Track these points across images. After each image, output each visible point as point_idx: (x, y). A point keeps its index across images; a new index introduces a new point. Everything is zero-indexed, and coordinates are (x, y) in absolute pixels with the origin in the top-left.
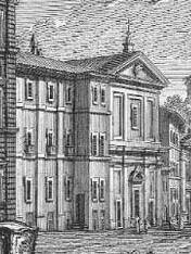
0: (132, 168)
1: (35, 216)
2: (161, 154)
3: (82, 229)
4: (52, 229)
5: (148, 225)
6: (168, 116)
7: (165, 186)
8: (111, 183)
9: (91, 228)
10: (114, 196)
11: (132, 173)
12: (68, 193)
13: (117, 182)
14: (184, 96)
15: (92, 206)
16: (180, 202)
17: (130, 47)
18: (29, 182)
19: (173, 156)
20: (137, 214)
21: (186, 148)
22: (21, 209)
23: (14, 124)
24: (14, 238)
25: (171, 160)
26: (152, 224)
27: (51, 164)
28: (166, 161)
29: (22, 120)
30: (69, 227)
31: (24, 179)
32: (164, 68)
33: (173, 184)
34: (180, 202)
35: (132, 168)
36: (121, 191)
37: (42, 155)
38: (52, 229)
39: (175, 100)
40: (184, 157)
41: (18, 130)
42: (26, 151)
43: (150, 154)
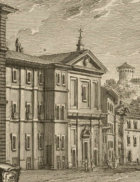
0: (83, 128)
1: (18, 159)
2: (104, 119)
3: (50, 169)
4: (30, 167)
5: (94, 166)
6: (107, 93)
7: (105, 139)
8: (69, 138)
9: (55, 168)
10: (71, 145)
11: (83, 131)
12: (40, 145)
13: (73, 136)
14: (117, 79)
15: (57, 153)
16: (115, 150)
17: (81, 47)
18: (14, 137)
19: (110, 119)
20: (86, 158)
21: (118, 114)
22: (10, 155)
23: (5, 98)
24: (4, 175)
25: (109, 122)
26: (96, 164)
27: (29, 125)
28: (105, 123)
29: (10, 95)
30: (42, 167)
31: (11, 135)
32: (103, 59)
33: (110, 138)
34: (115, 150)
35: (83, 128)
36: (76, 143)
37: (23, 119)
38: (30, 167)
39: (110, 82)
40: (117, 119)
41: (7, 102)
42: (13, 117)
43: (94, 118)
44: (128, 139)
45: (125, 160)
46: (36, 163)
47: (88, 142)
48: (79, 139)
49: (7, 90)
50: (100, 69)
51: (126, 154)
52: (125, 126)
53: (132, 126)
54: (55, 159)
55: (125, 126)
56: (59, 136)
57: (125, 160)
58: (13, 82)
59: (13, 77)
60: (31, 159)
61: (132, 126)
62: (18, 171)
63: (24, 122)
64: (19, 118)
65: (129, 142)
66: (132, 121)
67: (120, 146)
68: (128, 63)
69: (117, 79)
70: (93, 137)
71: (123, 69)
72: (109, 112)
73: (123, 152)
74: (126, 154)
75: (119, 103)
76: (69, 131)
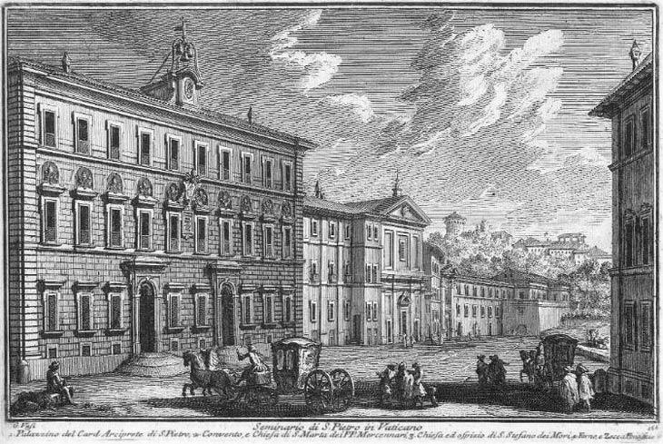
0: (400, 293)
1: (319, 333)
2: (425, 282)
3: (358, 344)
4: (333, 344)
5: (414, 341)
6: (430, 250)
7: (428, 309)
8: (383, 306)
9: (365, 343)
10: (385, 316)
11: (400, 297)
12: (347, 314)
13: (387, 305)
14: (443, 233)
15: (367, 325)
16: (441, 321)
17: (399, 192)
18: (314, 305)
19: (435, 283)
20: (405, 331)
21: (445, 276)
22: (307, 327)
23: (302, 256)
24: (301, 352)
25: (433, 286)
26: (417, 340)
27: (332, 290)
28: (429, 287)
29: (308, 252)
30: (348, 343)
31: (310, 302)
32: (427, 210)
33: (434, 306)
34: (441, 321)
35: (400, 293)
36: (391, 312)
37: (325, 282)
38: (333, 344)
39: (436, 237)
40: (443, 284)
41: (305, 261)
42: (312, 279)
43: (415, 282)
44: (458, 307)
45: (454, 335)
46: (341, 340)
47: (407, 311)
48: (395, 309)
49: (305, 245)
50: (422, 220)
51: (455, 327)
52: (454, 291)
53: (463, 291)
54: (365, 332)
55: (454, 291)
56: (370, 303)
57: (454, 335)
58: (312, 235)
59: (313, 229)
60: (335, 332)
61: (463, 291)
62: (319, 347)
63: (326, 285)
64: (321, 281)
65: (458, 312)
66: (463, 284)
67: (447, 316)
68: (458, 213)
69: (443, 233)
70: (413, 306)
71: (451, 220)
72: (433, 273)
73: (450, 325)
74: (455, 327)
75: (446, 262)
76: (383, 297)
